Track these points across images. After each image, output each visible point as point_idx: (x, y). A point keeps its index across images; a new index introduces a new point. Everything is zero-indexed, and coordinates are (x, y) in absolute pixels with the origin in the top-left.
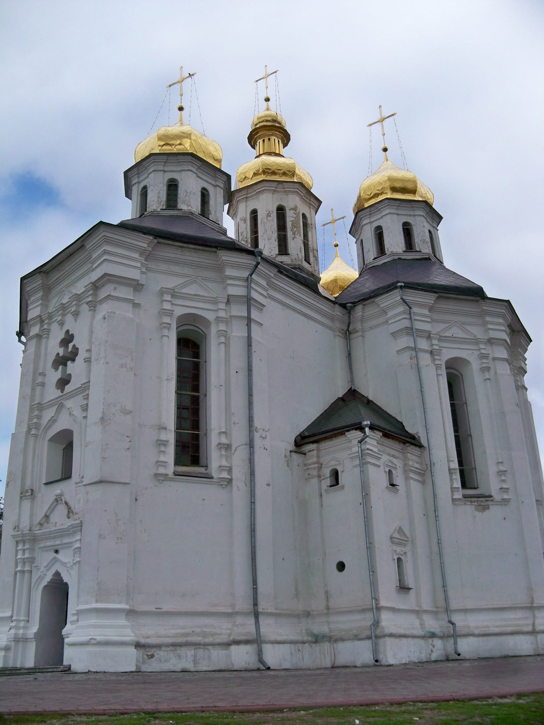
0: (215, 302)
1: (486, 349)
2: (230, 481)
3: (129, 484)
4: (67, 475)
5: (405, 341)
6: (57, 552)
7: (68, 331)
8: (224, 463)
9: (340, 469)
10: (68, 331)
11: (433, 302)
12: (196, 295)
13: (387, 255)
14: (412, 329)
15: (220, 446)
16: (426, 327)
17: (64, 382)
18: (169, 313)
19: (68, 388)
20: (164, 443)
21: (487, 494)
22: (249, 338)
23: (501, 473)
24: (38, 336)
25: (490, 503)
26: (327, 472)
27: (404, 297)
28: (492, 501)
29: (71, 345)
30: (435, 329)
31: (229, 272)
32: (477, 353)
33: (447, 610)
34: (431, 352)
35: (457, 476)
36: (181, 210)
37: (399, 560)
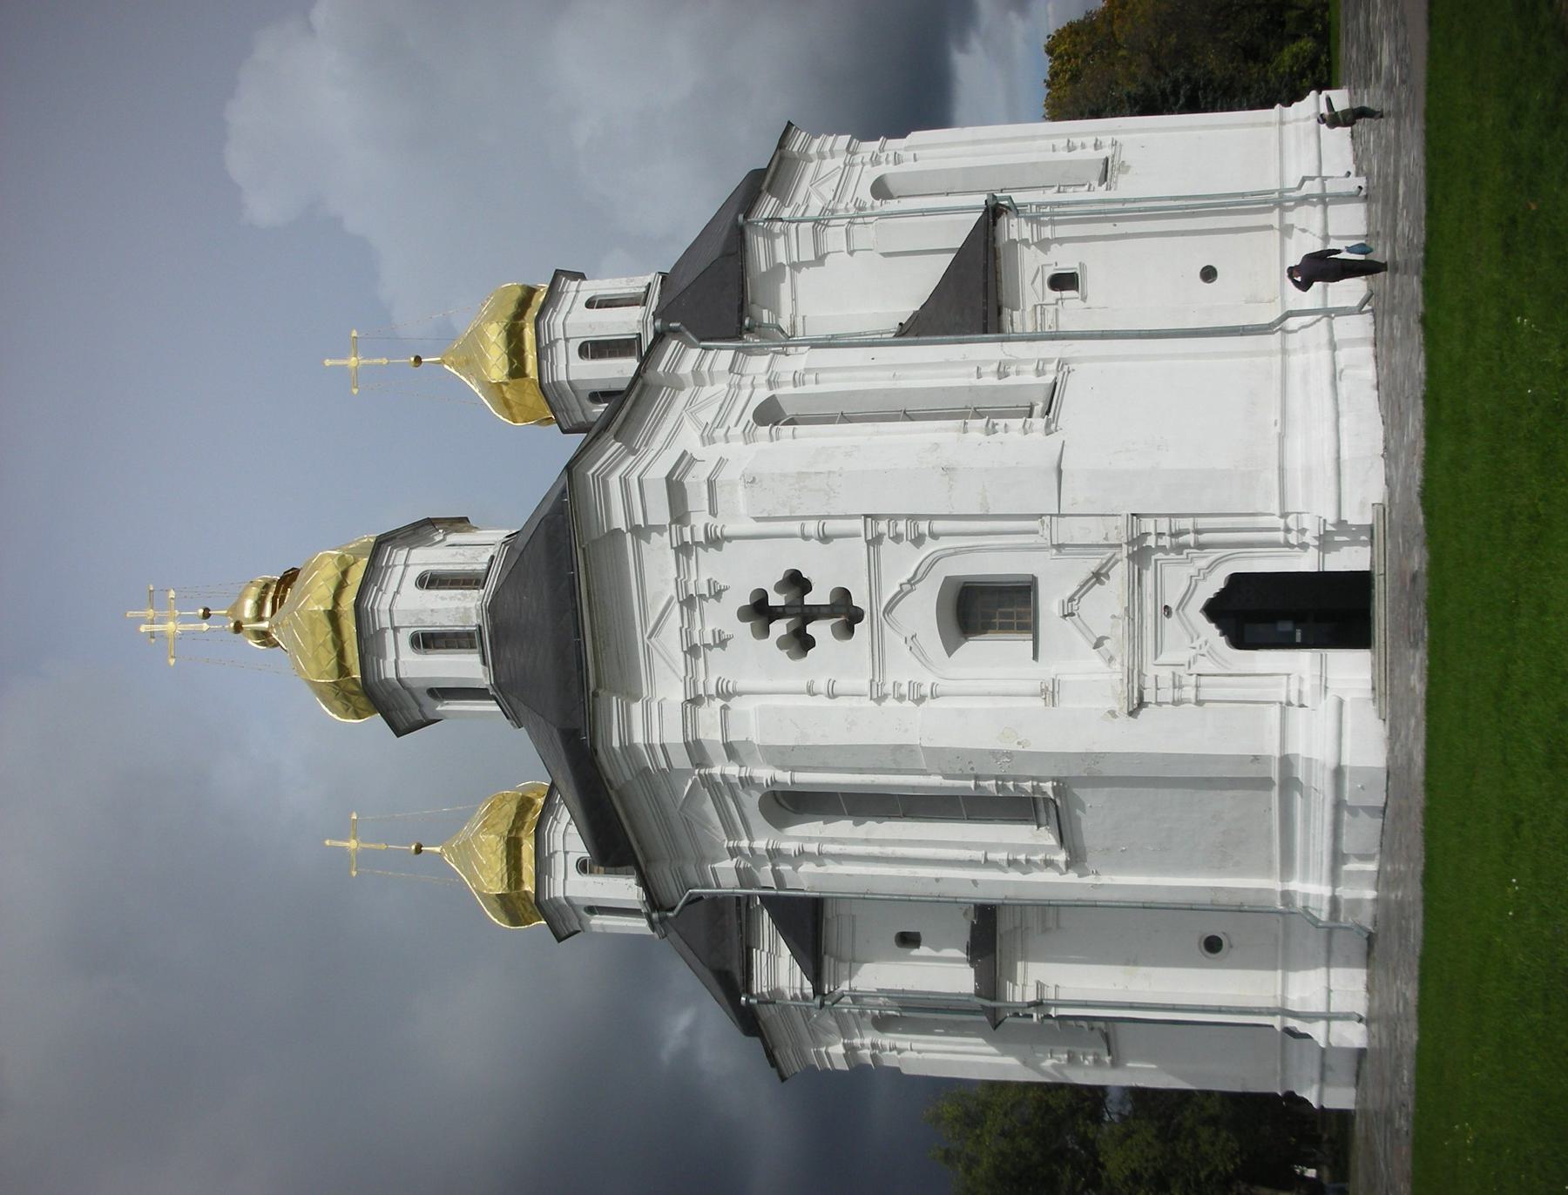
3: (1064, 442)
5: (834, 237)
6: (1167, 610)
9: (1050, 272)
11: (774, 199)
12: (721, 408)
13: (642, 332)
14: (816, 221)
17: (845, 613)
19: (859, 600)
21: (1101, 167)
25: (1116, 158)
27: (765, 216)
28: (1113, 156)
29: (776, 600)
32: (868, 167)
36: (492, 557)
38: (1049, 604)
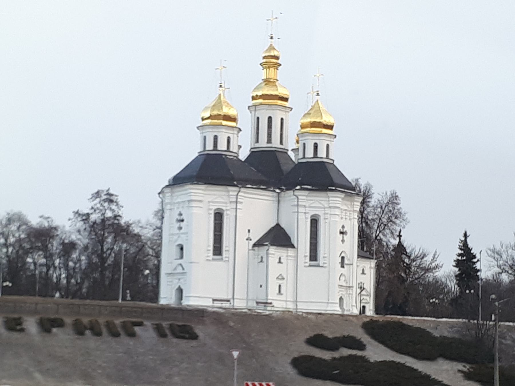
0: (226, 203)
1: (328, 211)
2: (228, 261)
4: (182, 257)
7: (180, 212)
8: (227, 256)
10: (180, 212)
15: (226, 251)
16: (304, 204)
18: (211, 209)
19: (182, 231)
20: (209, 250)
22: (236, 216)
23: (324, 257)
24: (171, 209)
26: (260, 257)
30: (307, 205)
31: (231, 193)
32: (323, 212)
33: (296, 301)
34: (305, 213)
35: (308, 258)
37: (280, 286)
38: (180, 261)
